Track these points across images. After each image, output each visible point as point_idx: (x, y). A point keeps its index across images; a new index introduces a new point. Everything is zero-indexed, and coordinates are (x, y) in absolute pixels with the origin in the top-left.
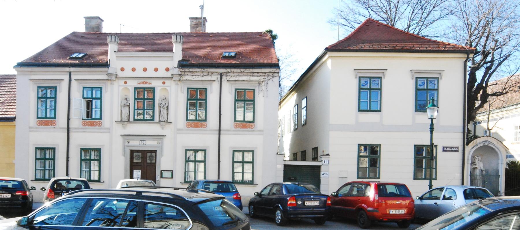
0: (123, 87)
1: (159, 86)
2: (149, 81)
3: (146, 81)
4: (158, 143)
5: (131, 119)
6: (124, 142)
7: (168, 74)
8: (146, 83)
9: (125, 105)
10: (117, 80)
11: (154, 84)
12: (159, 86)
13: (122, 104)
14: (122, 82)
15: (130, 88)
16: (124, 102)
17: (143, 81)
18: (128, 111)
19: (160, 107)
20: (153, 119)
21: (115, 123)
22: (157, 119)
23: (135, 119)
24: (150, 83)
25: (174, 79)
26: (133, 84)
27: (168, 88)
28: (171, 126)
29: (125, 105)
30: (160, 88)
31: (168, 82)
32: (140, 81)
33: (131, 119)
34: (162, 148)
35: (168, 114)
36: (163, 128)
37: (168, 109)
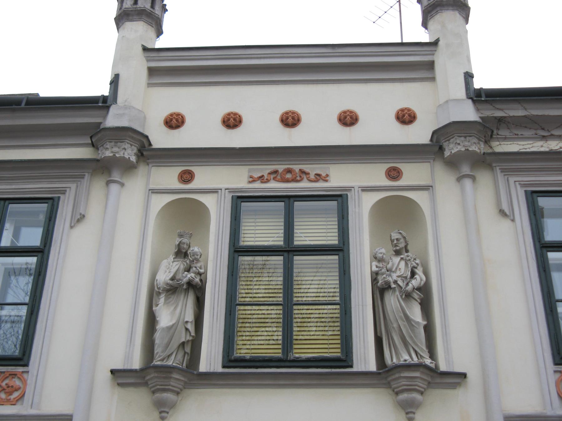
0: (168, 198)
1: (366, 189)
2: (313, 168)
5: (210, 358)
7: (419, 134)
9: (173, 289)
10: (142, 169)
11: (340, 176)
12: (366, 189)
13: (163, 277)
14: (167, 176)
15: (208, 201)
18: (190, 316)
19: (380, 290)
21: (104, 376)
22: (365, 358)
23: (230, 360)
24: (318, 177)
25: (452, 148)
28: (469, 398)
29: (173, 289)
30: (370, 200)
31: (413, 173)
32: (265, 169)
33: (210, 358)
35: (429, 330)
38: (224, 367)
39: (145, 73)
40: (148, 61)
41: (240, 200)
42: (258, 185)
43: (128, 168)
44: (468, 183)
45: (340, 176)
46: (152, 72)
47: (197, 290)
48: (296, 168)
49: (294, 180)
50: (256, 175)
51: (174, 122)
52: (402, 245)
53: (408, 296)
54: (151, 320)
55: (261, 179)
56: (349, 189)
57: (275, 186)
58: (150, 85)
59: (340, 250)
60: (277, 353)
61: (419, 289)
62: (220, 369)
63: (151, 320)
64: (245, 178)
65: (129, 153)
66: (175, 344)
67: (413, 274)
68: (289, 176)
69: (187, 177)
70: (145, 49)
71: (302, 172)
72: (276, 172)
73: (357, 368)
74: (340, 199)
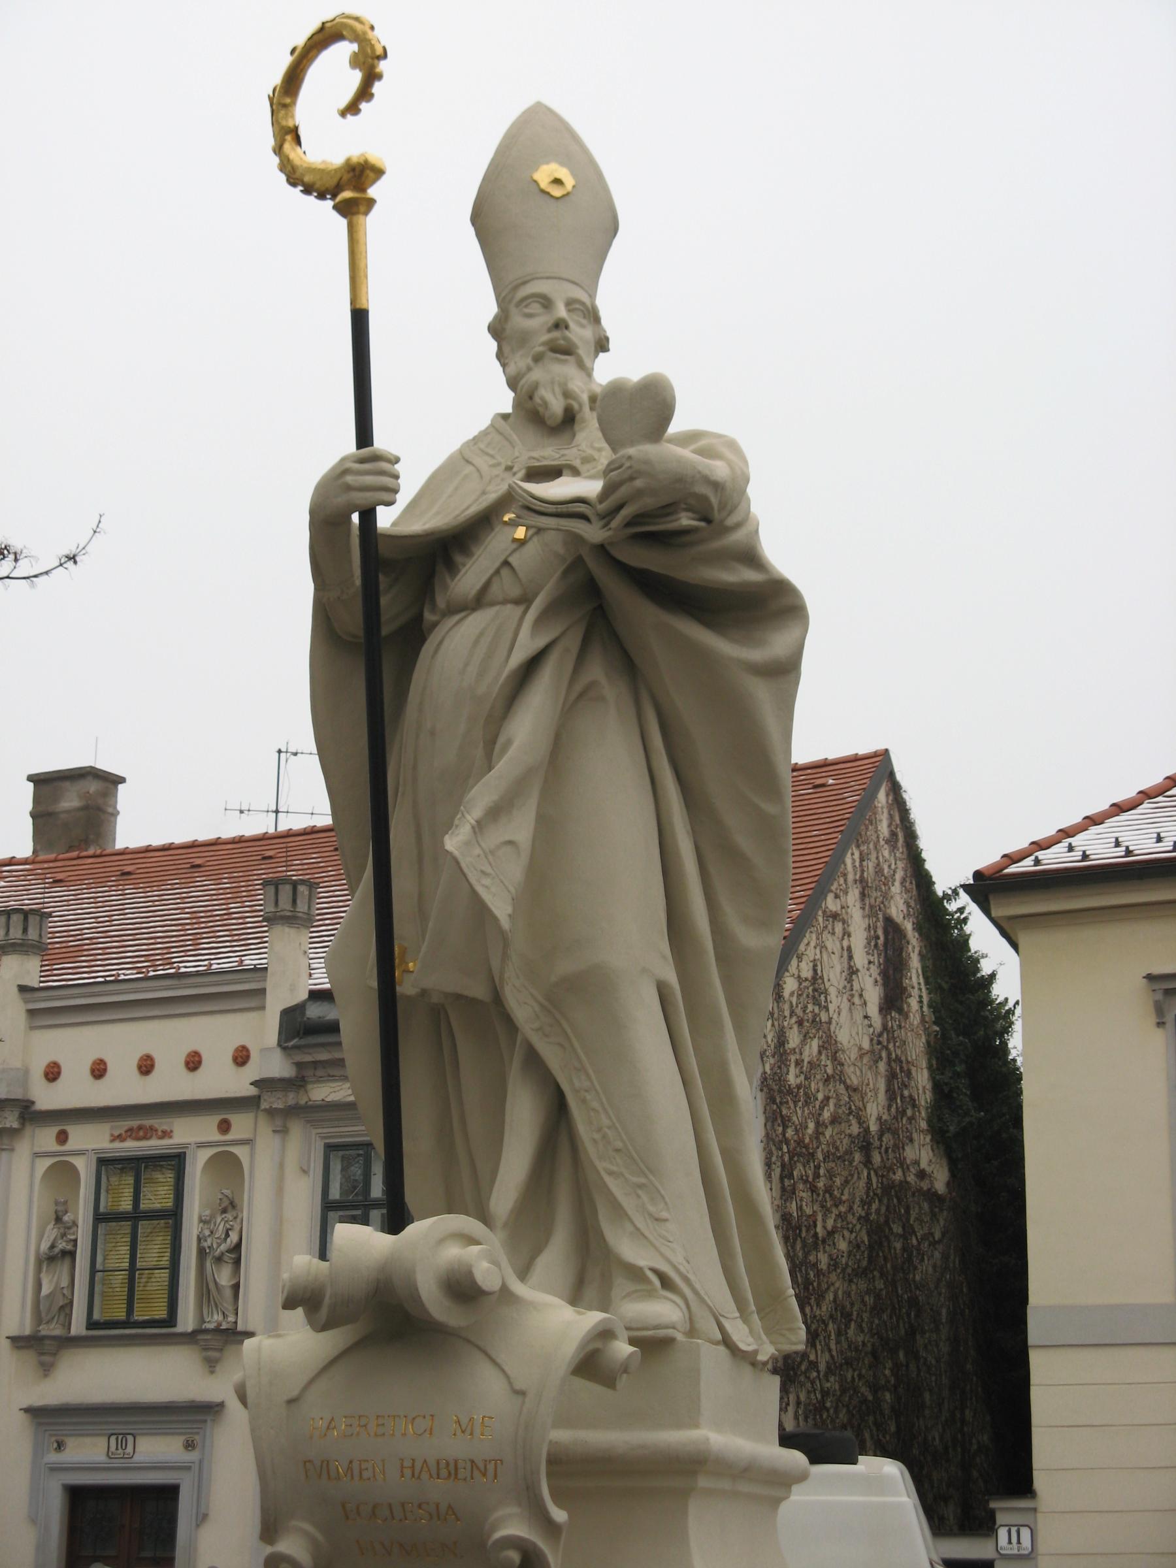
1: (202, 1145)
3: (147, 1122)
4: (189, 1446)
6: (38, 1451)
8: (146, 1133)
11: (183, 1132)
12: (202, 1145)
13: (44, 1246)
14: (46, 1138)
15: (80, 1163)
16: (51, 1233)
17: (134, 1123)
18: (65, 1283)
19: (202, 1253)
20: (171, 1320)
22: (187, 1320)
23: (92, 1325)
24: (166, 1134)
25: (264, 1105)
26: (91, 1140)
27: (241, 1152)
30: (204, 1155)
34: (201, 1471)
35: (236, 1287)
36: (211, 1365)
37: (237, 1262)
38: (87, 1329)
39: (22, 1018)
40: (26, 1001)
41: (105, 1163)
42: (117, 1145)
43: (13, 1133)
44: (277, 1139)
45: (183, 1132)
46: (32, 1013)
47: (71, 1255)
48: (147, 1122)
49: (145, 1138)
50: (116, 1134)
51: (53, 1073)
52: (226, 1203)
53: (219, 1260)
54: (38, 1285)
55: (119, 1137)
56: (186, 1146)
57: (131, 1146)
58: (32, 1028)
59: (173, 1216)
60: (121, 1315)
61: (229, 1251)
62: (83, 1332)
63: (38, 1285)
64: (108, 1137)
65: (11, 1120)
66: (55, 1308)
67: (227, 1235)
68: (141, 1133)
69: (62, 1137)
70: (23, 989)
71: (151, 1128)
72: (131, 1130)
73: (179, 1329)
74: (176, 1161)
